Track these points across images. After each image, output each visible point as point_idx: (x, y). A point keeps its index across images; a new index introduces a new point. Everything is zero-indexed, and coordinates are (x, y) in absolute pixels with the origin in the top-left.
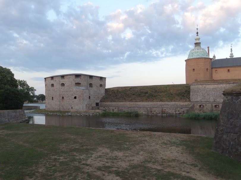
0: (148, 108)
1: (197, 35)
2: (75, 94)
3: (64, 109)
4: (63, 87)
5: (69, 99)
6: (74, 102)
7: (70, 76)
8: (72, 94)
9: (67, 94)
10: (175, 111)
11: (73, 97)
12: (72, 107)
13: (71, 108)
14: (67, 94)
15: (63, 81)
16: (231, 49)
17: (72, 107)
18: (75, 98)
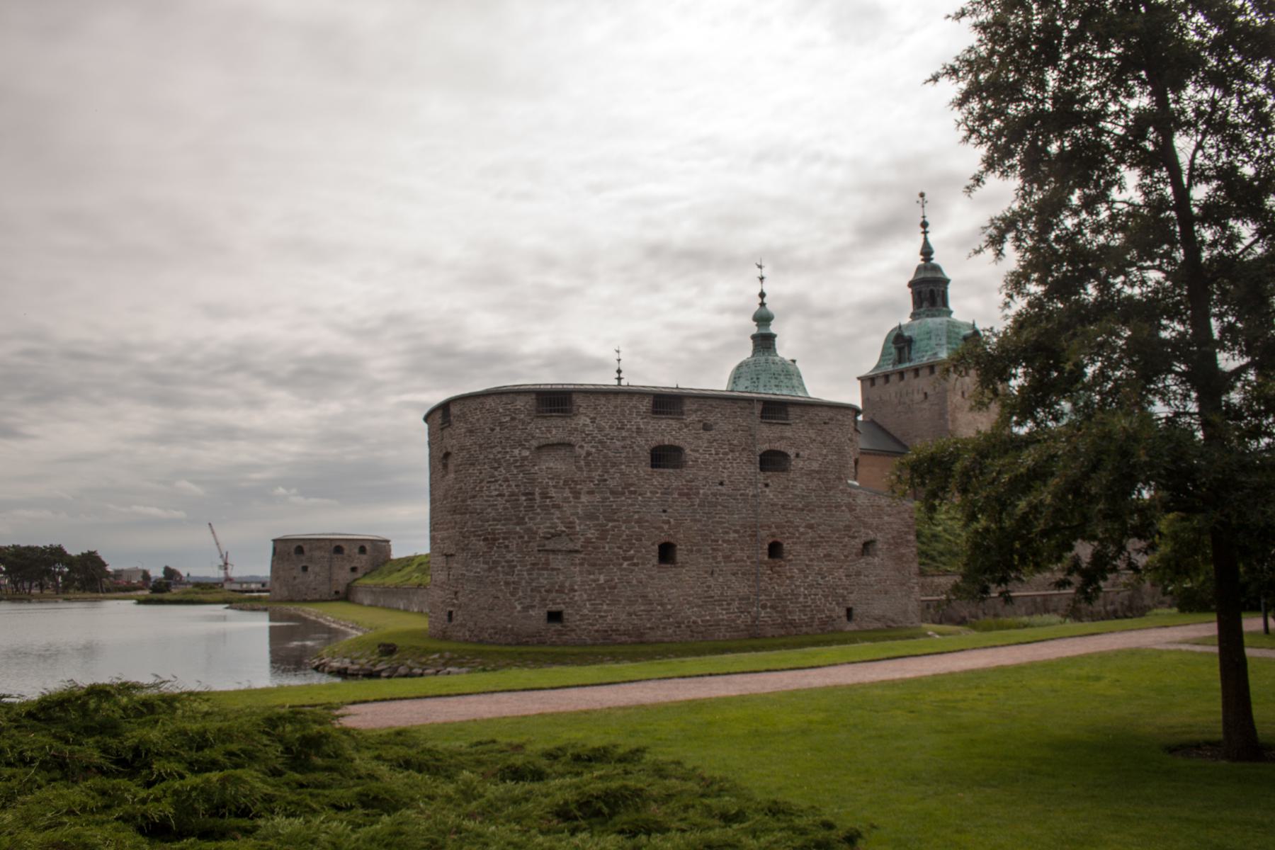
0: (1039, 599)
1: (762, 304)
2: (865, 525)
3: (792, 623)
4: (776, 479)
5: (827, 556)
6: (858, 574)
7: (831, 413)
8: (848, 528)
9: (811, 527)
10: (1105, 606)
11: (858, 543)
12: (849, 611)
13: (843, 613)
14: (811, 527)
15: (782, 438)
16: (619, 371)
17: (849, 611)
18: (867, 547)
